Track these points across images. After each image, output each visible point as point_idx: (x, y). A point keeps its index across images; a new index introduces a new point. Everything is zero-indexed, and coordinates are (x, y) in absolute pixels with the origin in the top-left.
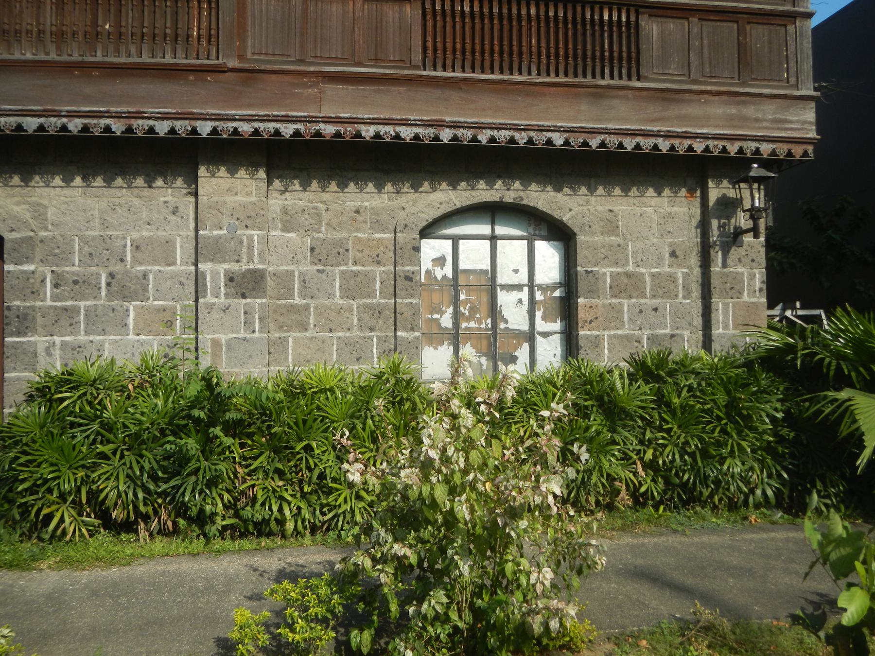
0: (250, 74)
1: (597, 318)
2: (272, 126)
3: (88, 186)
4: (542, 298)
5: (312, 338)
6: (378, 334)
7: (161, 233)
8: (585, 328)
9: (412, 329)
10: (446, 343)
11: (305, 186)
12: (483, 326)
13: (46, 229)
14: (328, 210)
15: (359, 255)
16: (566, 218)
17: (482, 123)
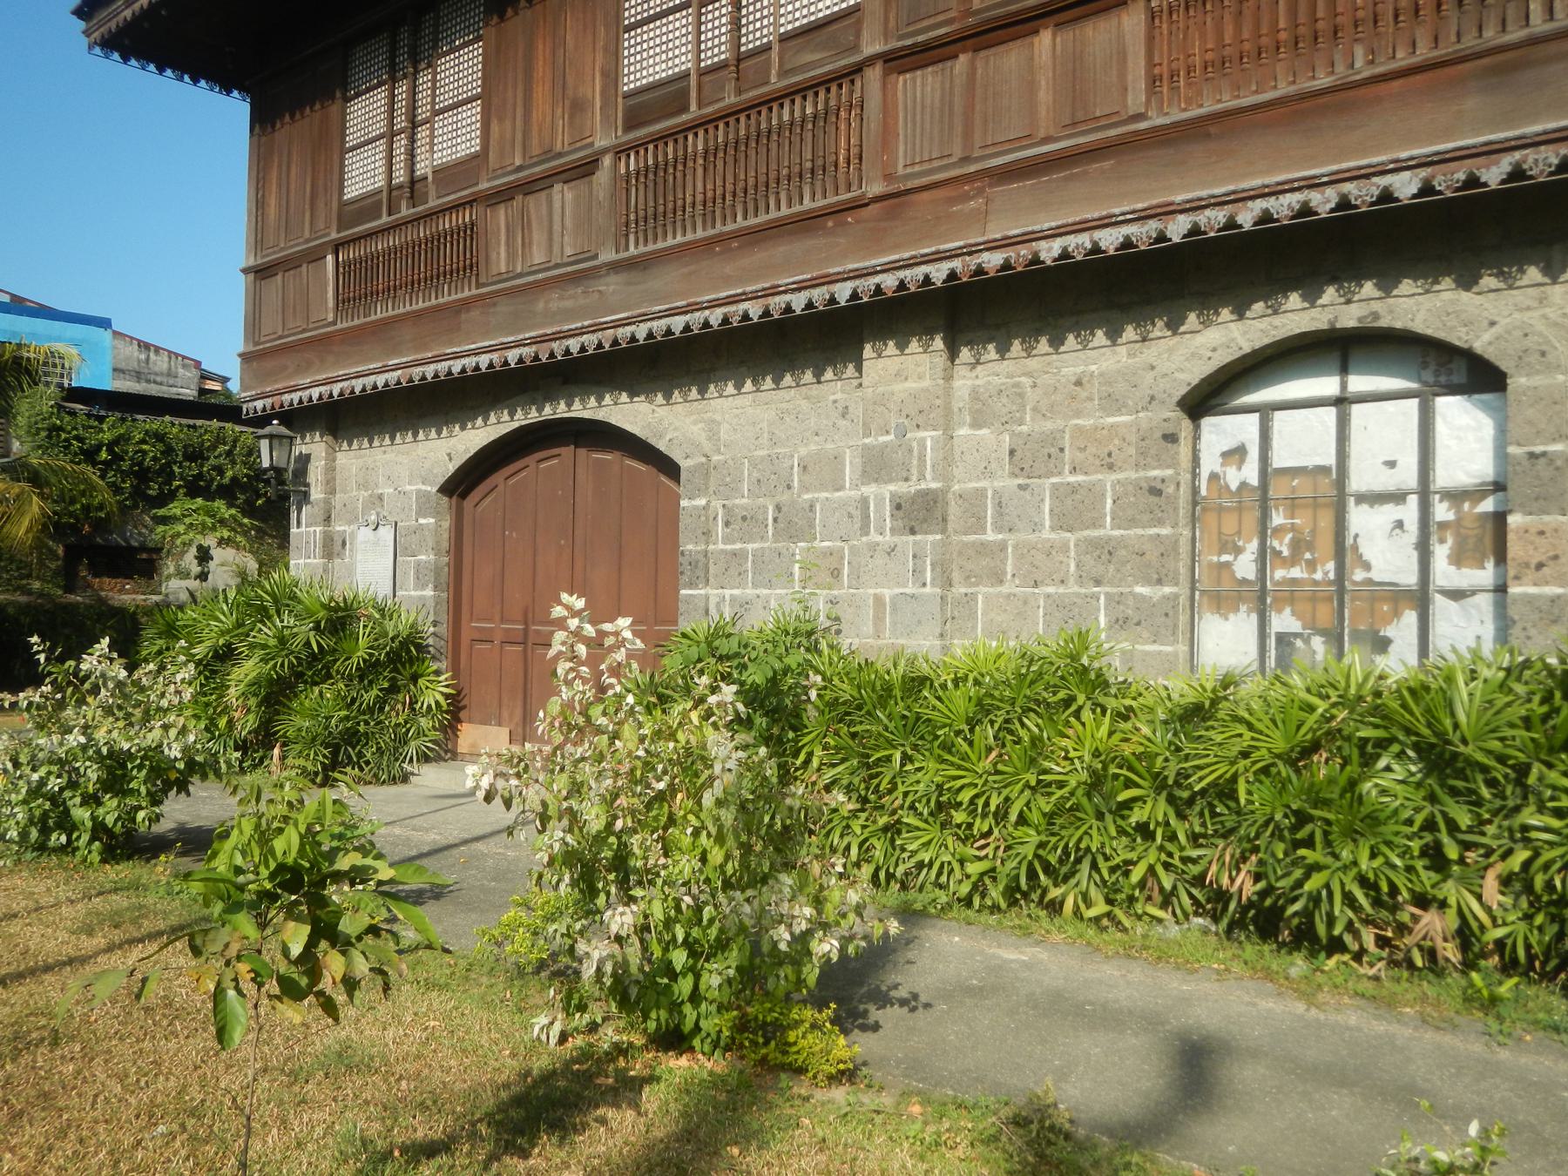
0: (895, 198)
1: (1556, 557)
2: (921, 271)
3: (758, 390)
4: (1451, 516)
5: (1008, 596)
6: (1108, 589)
7: (830, 446)
8: (1525, 579)
9: (1160, 582)
10: (1243, 608)
11: (1003, 350)
12: (1318, 576)
13: (719, 452)
14: (1035, 386)
15: (1080, 456)
16: (1481, 344)
17: (1244, 191)
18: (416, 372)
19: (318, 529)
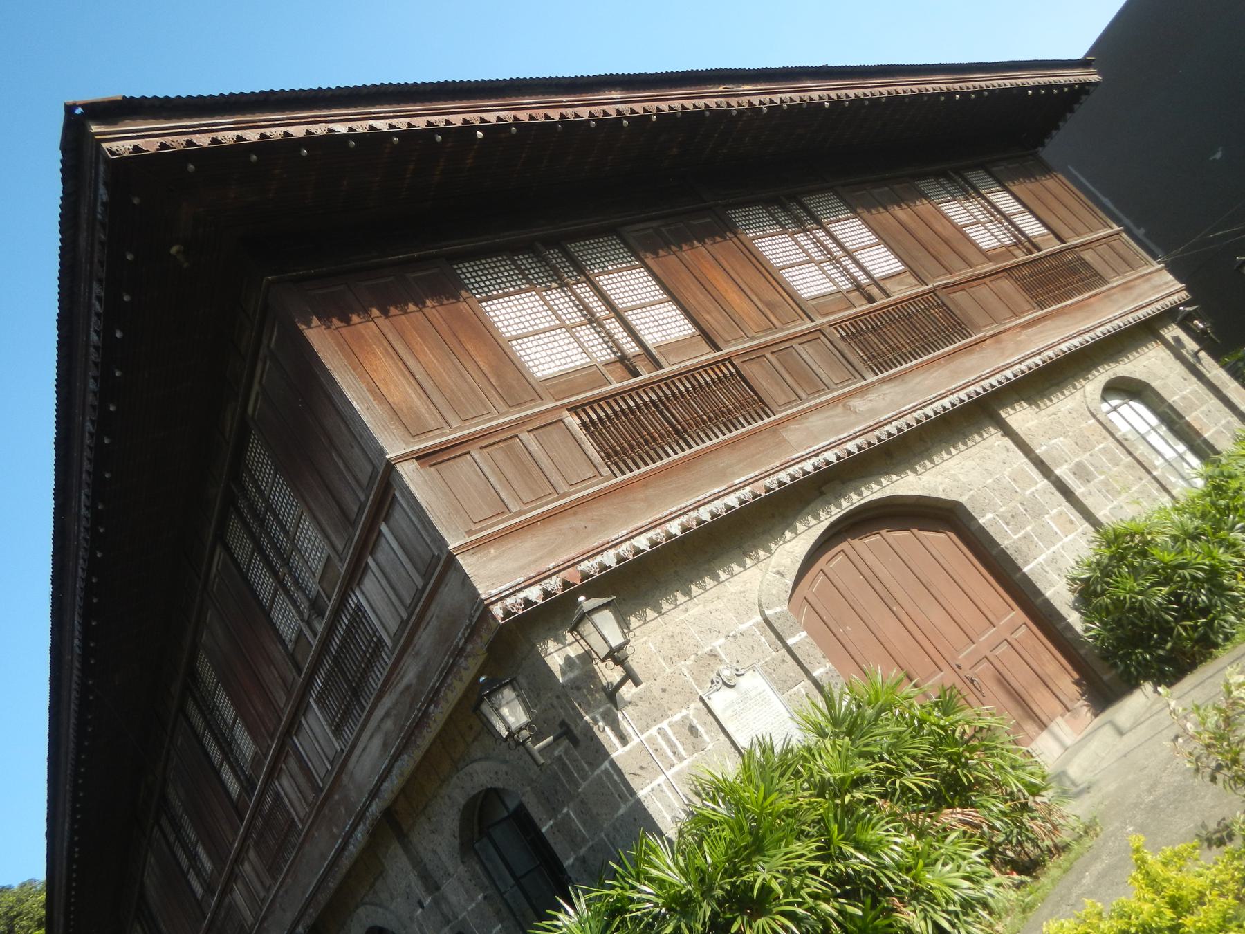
18: (771, 482)
19: (664, 724)
